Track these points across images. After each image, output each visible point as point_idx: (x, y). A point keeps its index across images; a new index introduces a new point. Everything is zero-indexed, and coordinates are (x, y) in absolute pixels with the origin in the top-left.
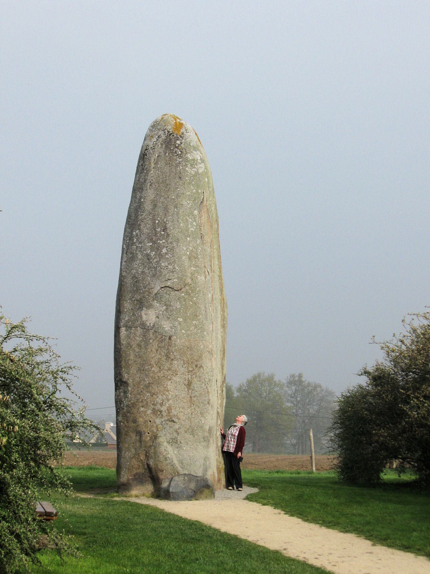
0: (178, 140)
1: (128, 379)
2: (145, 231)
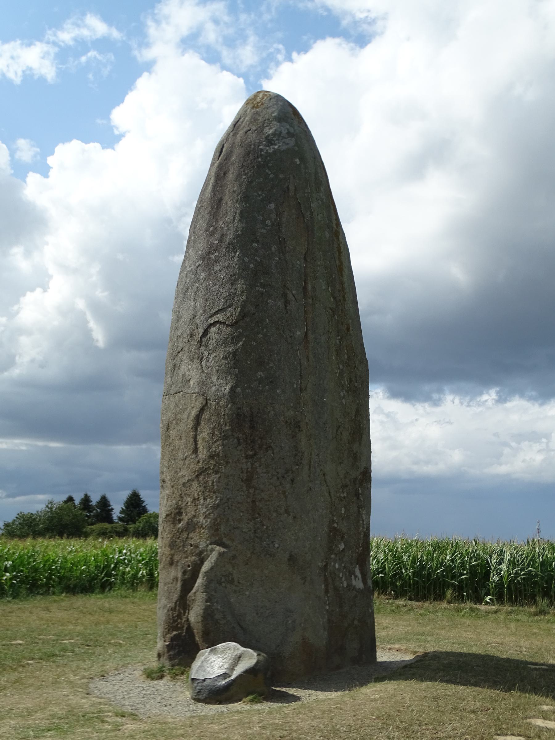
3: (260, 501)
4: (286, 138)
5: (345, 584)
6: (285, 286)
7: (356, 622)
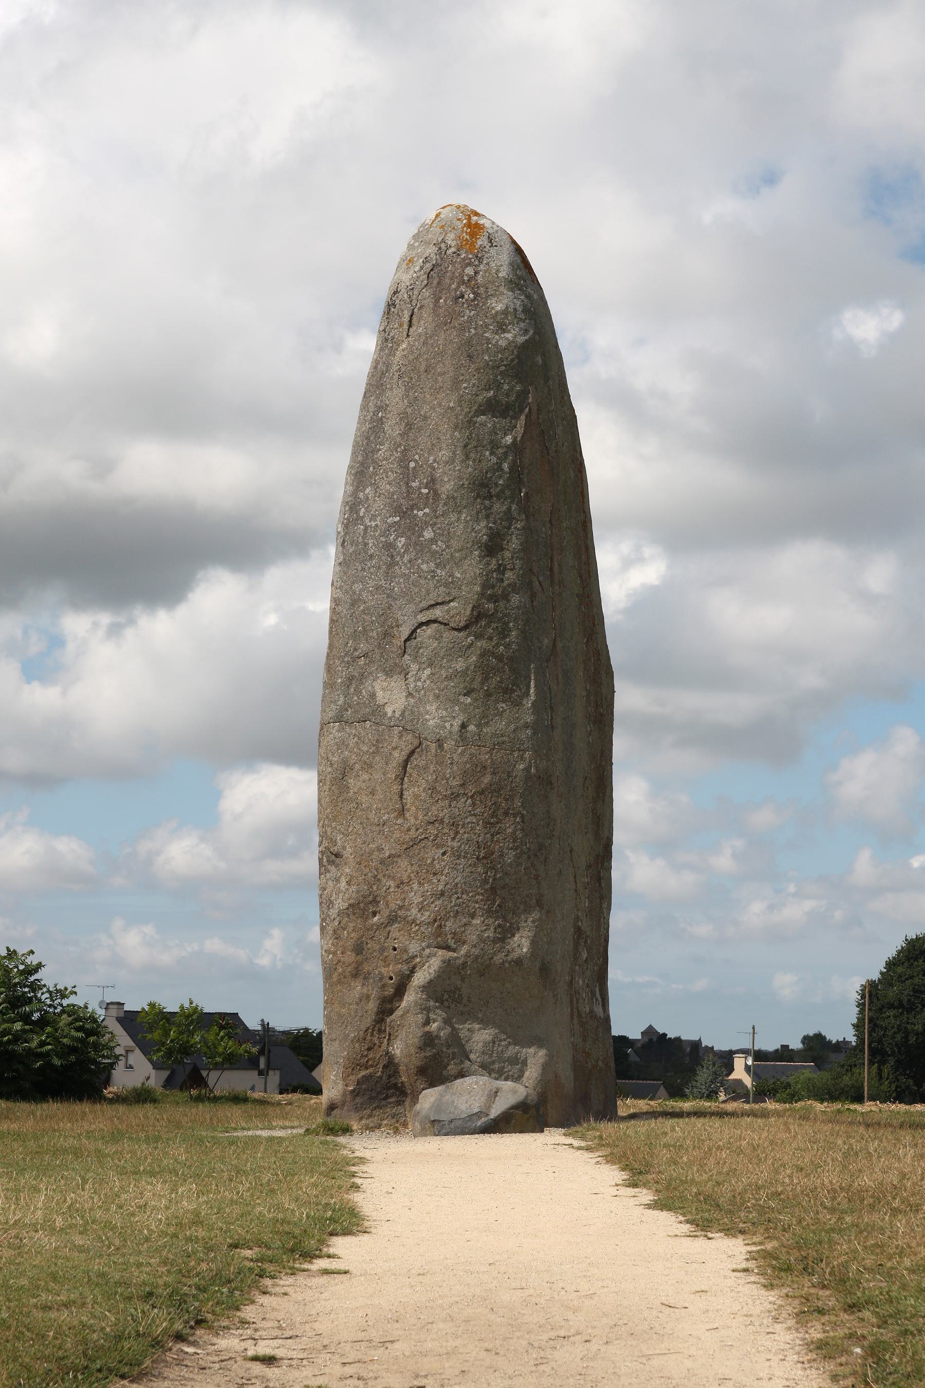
0: (469, 264)
1: (344, 848)
2: (385, 487)
3: (503, 888)
5: (587, 1010)
6: (531, 570)
7: (600, 1063)
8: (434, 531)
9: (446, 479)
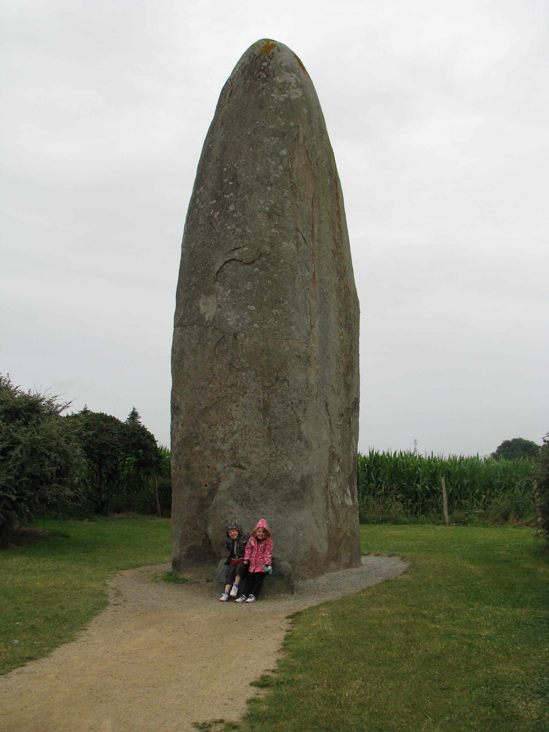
1: (181, 404)
3: (276, 428)
4: (295, 89)
5: (340, 502)
6: (297, 229)
7: (348, 534)
8: (235, 206)
9: (243, 175)
